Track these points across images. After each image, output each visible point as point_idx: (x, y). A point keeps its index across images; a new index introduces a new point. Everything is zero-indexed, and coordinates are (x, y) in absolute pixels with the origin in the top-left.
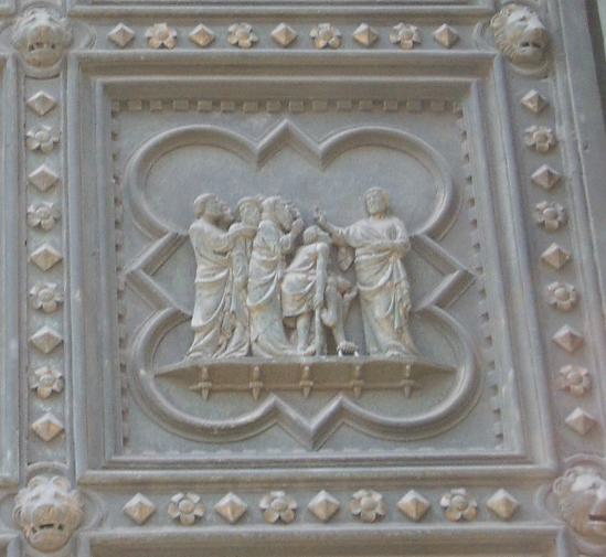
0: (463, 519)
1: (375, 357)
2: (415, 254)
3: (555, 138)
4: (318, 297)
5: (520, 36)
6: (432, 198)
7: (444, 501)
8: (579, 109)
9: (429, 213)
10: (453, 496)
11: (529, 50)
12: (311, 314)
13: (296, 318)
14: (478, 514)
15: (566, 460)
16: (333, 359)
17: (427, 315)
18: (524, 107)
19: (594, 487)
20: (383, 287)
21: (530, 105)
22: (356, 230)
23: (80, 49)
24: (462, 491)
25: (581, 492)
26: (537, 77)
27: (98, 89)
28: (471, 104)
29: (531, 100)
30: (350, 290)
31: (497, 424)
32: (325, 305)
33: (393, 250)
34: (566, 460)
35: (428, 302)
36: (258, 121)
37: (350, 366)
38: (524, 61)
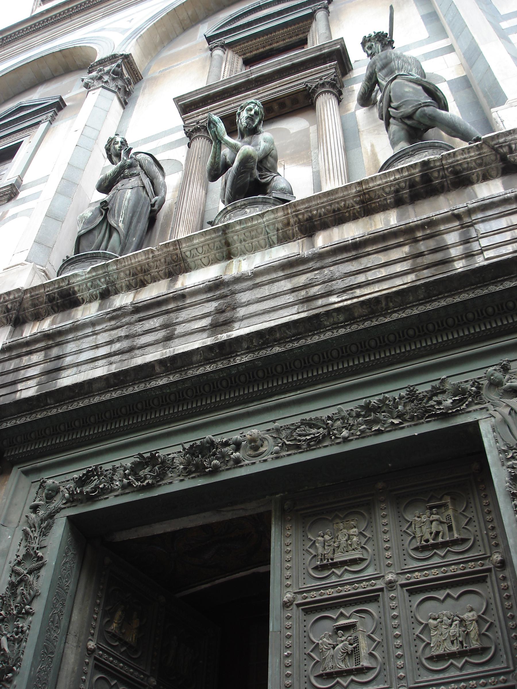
0: (494, 685)
1: (473, 647)
2: (480, 620)
4: (458, 635)
6: (482, 604)
7: (490, 681)
9: (482, 608)
11: (499, 565)
12: (457, 639)
13: (454, 641)
14: (497, 683)
16: (462, 649)
17: (484, 634)
20: (473, 628)
22: (465, 616)
23: (400, 582)
24: (493, 678)
26: (502, 570)
27: (405, 591)
30: (465, 631)
32: (459, 636)
33: (473, 620)
36: (442, 592)
37: (467, 651)
38: (498, 567)
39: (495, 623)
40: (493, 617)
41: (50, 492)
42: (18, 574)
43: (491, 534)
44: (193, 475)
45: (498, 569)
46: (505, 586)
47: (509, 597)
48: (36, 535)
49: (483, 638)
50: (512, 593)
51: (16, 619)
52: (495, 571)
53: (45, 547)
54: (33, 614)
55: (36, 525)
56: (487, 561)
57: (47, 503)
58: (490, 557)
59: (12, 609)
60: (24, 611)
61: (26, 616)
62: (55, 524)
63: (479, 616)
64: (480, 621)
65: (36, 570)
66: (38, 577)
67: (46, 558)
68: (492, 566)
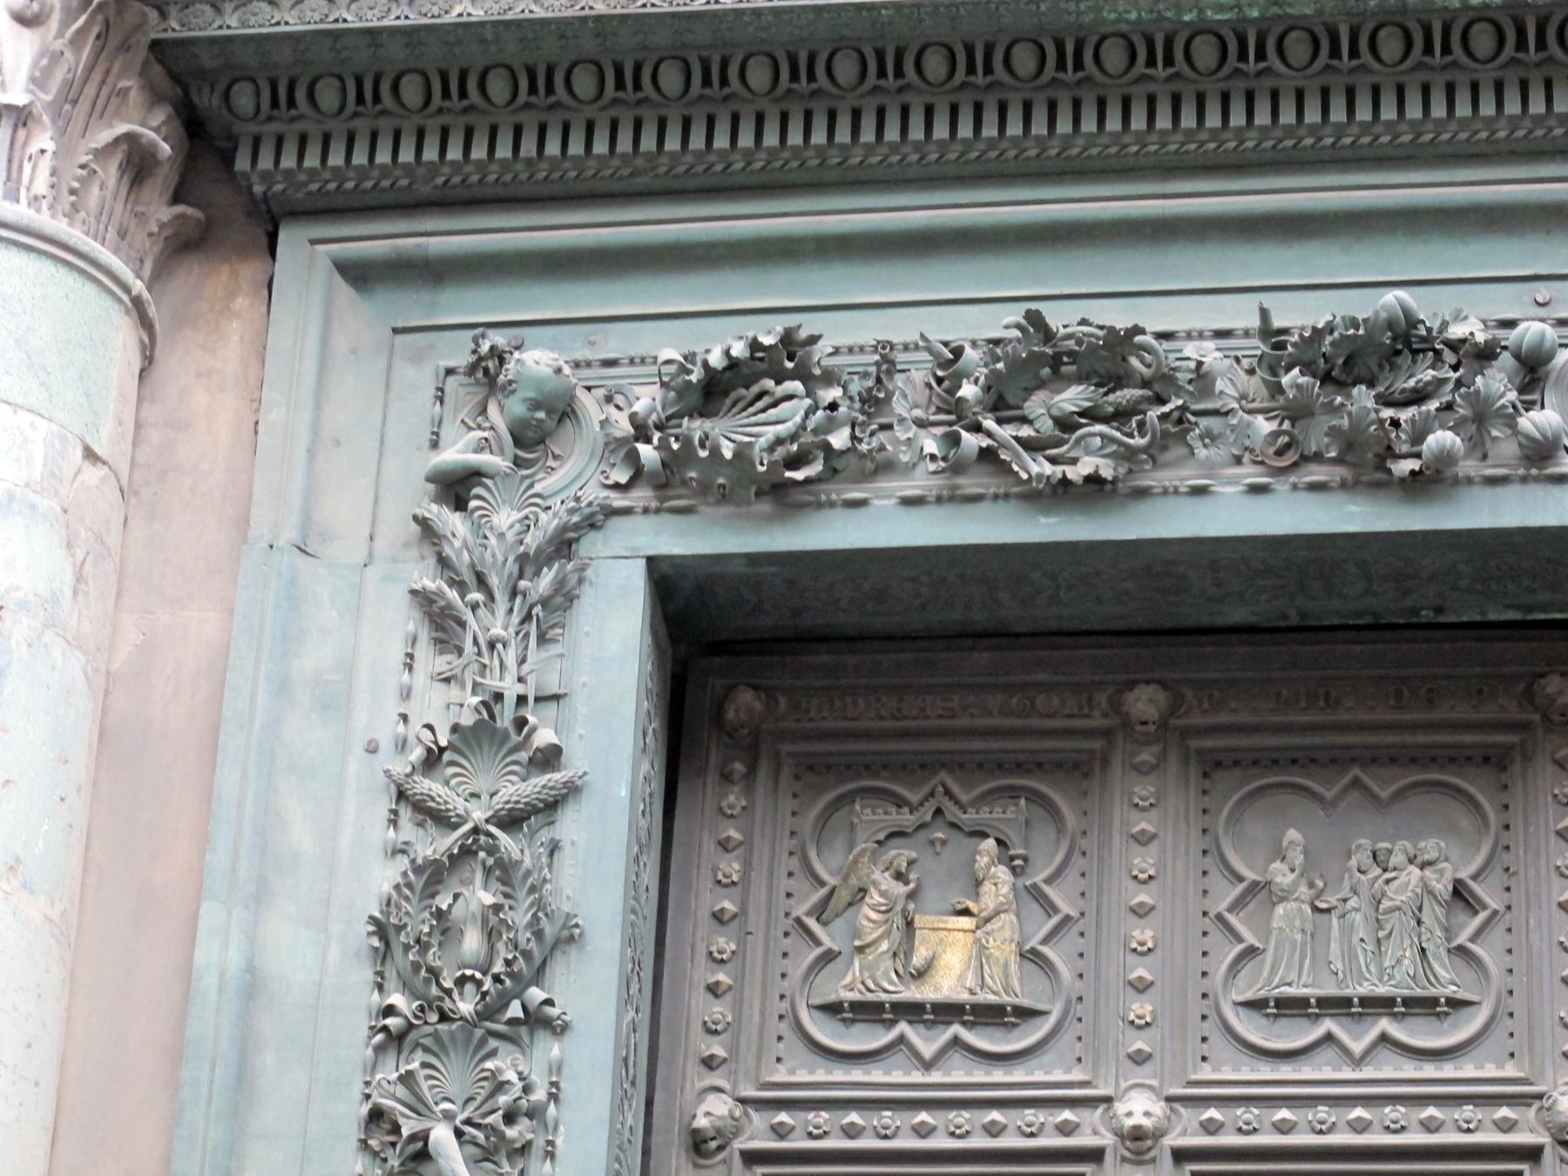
41: (541, 415)
42: (436, 817)
44: (1317, 473)
48: (497, 631)
51: (482, 1043)
53: (556, 698)
54: (565, 1027)
55: (494, 581)
57: (518, 463)
59: (448, 992)
60: (515, 1010)
61: (523, 1031)
62: (586, 588)
65: (537, 811)
66: (554, 848)
67: (575, 764)
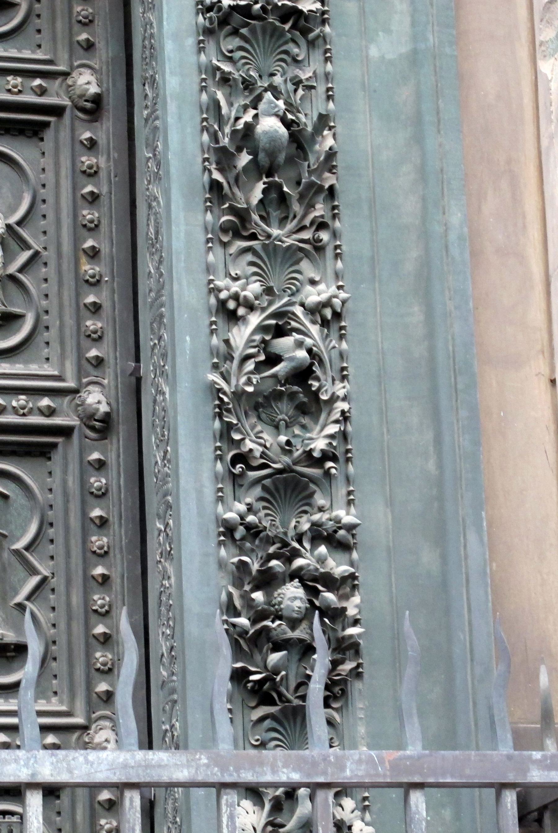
0: (24, 415)
3: (98, 167)
5: (84, 95)
7: (14, 404)
8: (114, 148)
10: (18, 401)
14: (31, 412)
15: (85, 380)
17: (12, 278)
18: (81, 142)
19: (99, 402)
21: (85, 142)
25: (90, 405)
28: (49, 135)
29: (86, 140)
31: (46, 350)
34: (85, 380)
35: (12, 269)
38: (83, 110)
39: (44, 253)
40: (43, 238)
43: (79, 9)
45: (80, 115)
46: (91, 167)
47: (94, 198)
49: (12, 287)
50: (105, 190)
52: (74, 118)
56: (58, 82)
58: (66, 75)
63: (9, 227)
64: (13, 244)
68: (66, 102)
